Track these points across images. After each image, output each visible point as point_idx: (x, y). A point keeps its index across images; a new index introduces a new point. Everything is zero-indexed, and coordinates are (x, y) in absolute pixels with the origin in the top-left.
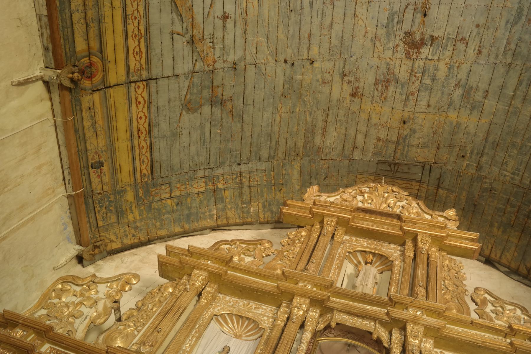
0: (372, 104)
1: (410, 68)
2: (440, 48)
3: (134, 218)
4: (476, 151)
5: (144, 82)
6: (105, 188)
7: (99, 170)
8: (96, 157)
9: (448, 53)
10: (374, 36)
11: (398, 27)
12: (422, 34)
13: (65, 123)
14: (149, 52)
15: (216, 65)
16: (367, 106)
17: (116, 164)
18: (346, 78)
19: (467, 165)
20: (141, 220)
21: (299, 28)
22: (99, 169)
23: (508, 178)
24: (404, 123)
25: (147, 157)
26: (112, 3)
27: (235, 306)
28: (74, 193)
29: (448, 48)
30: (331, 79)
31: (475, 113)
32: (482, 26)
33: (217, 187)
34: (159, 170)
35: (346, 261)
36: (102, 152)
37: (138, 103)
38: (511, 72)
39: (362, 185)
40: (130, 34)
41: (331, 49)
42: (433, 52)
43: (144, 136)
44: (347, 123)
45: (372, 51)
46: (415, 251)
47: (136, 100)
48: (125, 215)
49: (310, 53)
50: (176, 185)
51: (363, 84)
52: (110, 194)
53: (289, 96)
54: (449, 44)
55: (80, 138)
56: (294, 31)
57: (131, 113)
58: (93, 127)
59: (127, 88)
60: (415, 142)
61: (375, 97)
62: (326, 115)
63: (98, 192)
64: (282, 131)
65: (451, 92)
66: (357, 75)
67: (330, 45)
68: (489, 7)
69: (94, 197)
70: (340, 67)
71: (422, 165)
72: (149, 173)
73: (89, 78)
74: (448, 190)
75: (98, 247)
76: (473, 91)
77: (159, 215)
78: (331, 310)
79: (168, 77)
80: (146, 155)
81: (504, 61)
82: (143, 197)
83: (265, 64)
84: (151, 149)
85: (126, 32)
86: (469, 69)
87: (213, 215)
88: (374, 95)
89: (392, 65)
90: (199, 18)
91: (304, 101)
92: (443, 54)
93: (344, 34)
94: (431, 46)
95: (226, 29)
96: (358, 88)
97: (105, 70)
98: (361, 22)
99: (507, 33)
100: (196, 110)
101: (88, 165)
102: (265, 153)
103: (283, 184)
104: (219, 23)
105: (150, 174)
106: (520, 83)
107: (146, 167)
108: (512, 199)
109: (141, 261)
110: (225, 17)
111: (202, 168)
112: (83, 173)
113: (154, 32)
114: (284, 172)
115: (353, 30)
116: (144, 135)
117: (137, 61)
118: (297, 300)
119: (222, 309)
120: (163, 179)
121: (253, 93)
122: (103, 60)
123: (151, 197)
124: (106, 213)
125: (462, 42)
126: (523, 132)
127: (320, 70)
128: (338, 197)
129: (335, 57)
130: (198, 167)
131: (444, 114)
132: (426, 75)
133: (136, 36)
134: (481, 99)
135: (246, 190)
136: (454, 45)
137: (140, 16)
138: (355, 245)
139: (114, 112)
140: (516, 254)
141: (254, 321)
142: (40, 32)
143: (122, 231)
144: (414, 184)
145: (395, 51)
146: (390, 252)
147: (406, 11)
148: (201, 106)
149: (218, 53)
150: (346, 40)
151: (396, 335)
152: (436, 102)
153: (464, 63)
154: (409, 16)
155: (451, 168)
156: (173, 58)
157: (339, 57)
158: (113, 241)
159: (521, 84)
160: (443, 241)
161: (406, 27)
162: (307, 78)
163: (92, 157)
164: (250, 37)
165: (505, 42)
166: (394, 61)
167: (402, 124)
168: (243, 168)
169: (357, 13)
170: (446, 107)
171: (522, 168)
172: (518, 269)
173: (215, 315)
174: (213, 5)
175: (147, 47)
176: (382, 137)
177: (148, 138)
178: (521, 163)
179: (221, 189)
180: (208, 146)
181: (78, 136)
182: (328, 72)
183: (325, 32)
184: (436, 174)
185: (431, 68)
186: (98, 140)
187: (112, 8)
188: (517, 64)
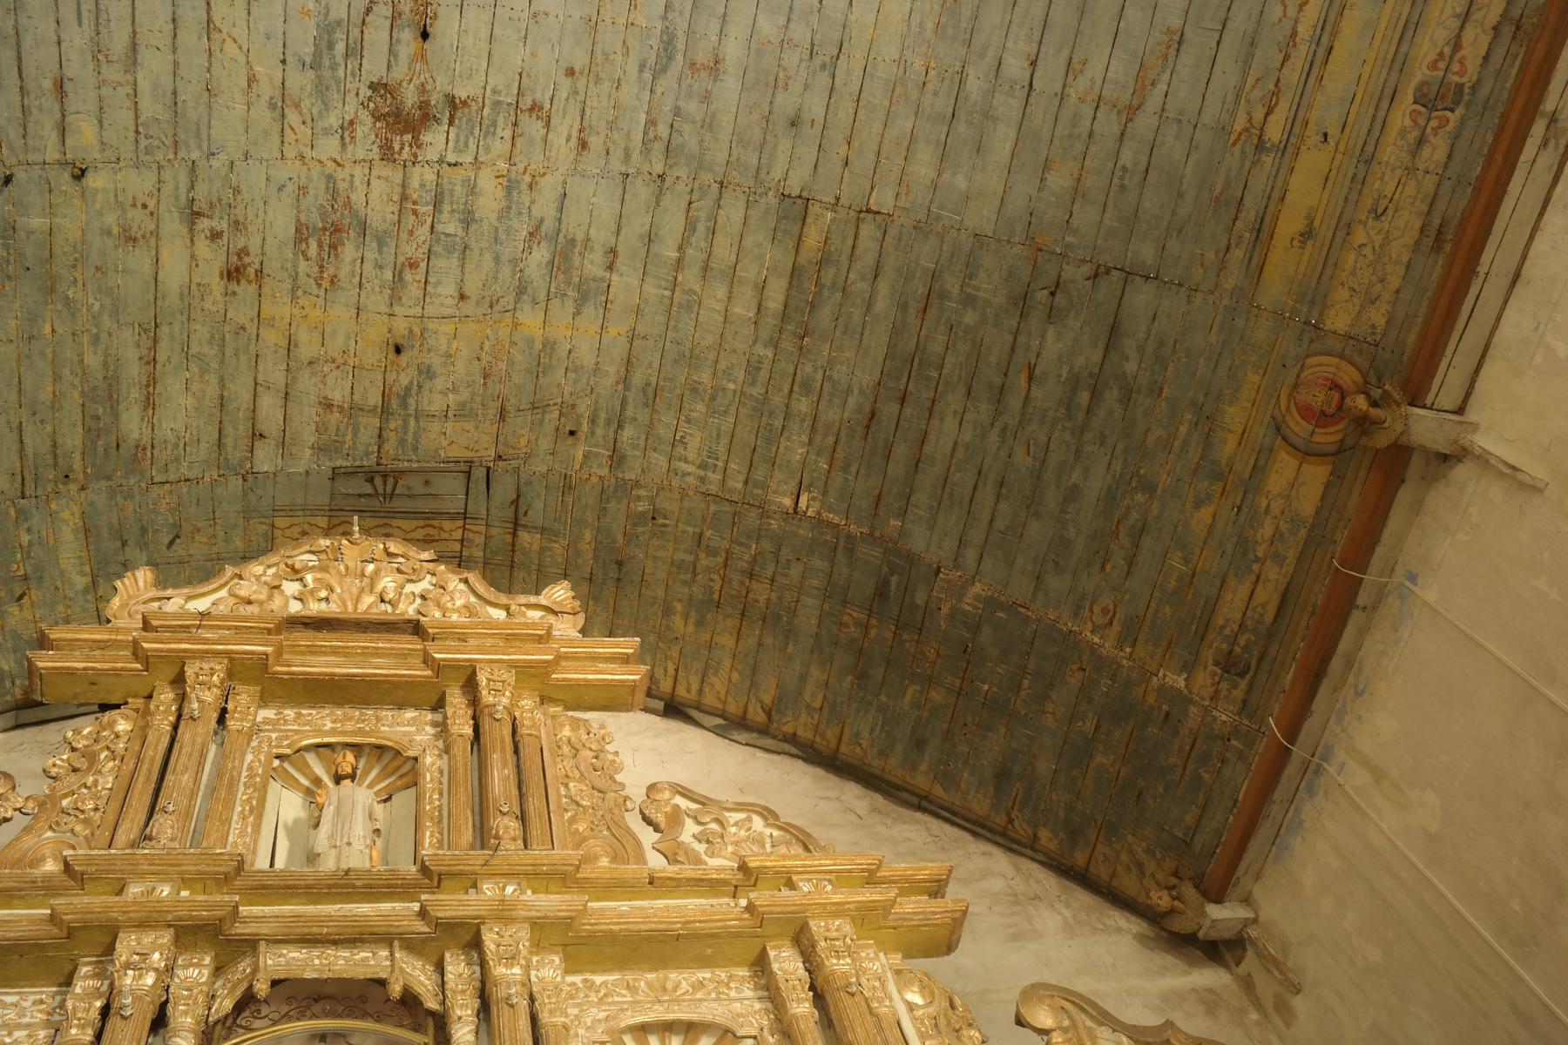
0: (294, 299)
1: (398, 190)
2: (477, 132)
4: (603, 415)
9: (499, 146)
10: (278, 93)
11: (349, 66)
12: (422, 89)
16: (279, 307)
18: (204, 224)
23: (690, 479)
24: (398, 350)
29: (499, 132)
30: (152, 227)
31: (591, 312)
32: (581, 73)
35: (275, 787)
38: (667, 200)
39: (294, 549)
41: (141, 129)
42: (457, 141)
44: (222, 362)
45: (276, 140)
46: (474, 718)
49: (69, 142)
54: (501, 120)
60: (437, 404)
61: (302, 279)
62: (150, 343)
65: (520, 255)
66: (237, 211)
67: (137, 117)
68: (593, 23)
70: (177, 188)
71: (464, 467)
74: (543, 530)
76: (576, 251)
78: (250, 945)
81: (646, 168)
86: (561, 190)
88: (297, 273)
89: (344, 180)
91: (67, 302)
92: (488, 150)
93: (180, 86)
94: (451, 124)
96: (244, 252)
98: (231, 48)
99: (646, 95)
103: (26, 578)
106: (690, 226)
108: (708, 533)
114: (25, 538)
115: (209, 71)
118: (127, 946)
125: (534, 116)
126: (712, 356)
127: (112, 200)
128: (223, 593)
129: (160, 157)
132: (446, 207)
134: (600, 273)
136: (515, 125)
138: (296, 732)
140: (735, 676)
144: (447, 525)
145: (348, 139)
146: (405, 734)
147: (368, 19)
150: (190, 104)
151: (458, 968)
152: (480, 286)
153: (545, 174)
154: (377, 35)
157: (171, 156)
159: (695, 230)
160: (548, 674)
161: (374, 67)
165: (643, 117)
166: (348, 170)
167: (392, 355)
169: (216, 18)
170: (509, 300)
171: (722, 449)
176: (337, 396)
178: (718, 435)
182: (139, 205)
183: (112, 73)
184: (504, 490)
185: (458, 188)
188: (678, 178)
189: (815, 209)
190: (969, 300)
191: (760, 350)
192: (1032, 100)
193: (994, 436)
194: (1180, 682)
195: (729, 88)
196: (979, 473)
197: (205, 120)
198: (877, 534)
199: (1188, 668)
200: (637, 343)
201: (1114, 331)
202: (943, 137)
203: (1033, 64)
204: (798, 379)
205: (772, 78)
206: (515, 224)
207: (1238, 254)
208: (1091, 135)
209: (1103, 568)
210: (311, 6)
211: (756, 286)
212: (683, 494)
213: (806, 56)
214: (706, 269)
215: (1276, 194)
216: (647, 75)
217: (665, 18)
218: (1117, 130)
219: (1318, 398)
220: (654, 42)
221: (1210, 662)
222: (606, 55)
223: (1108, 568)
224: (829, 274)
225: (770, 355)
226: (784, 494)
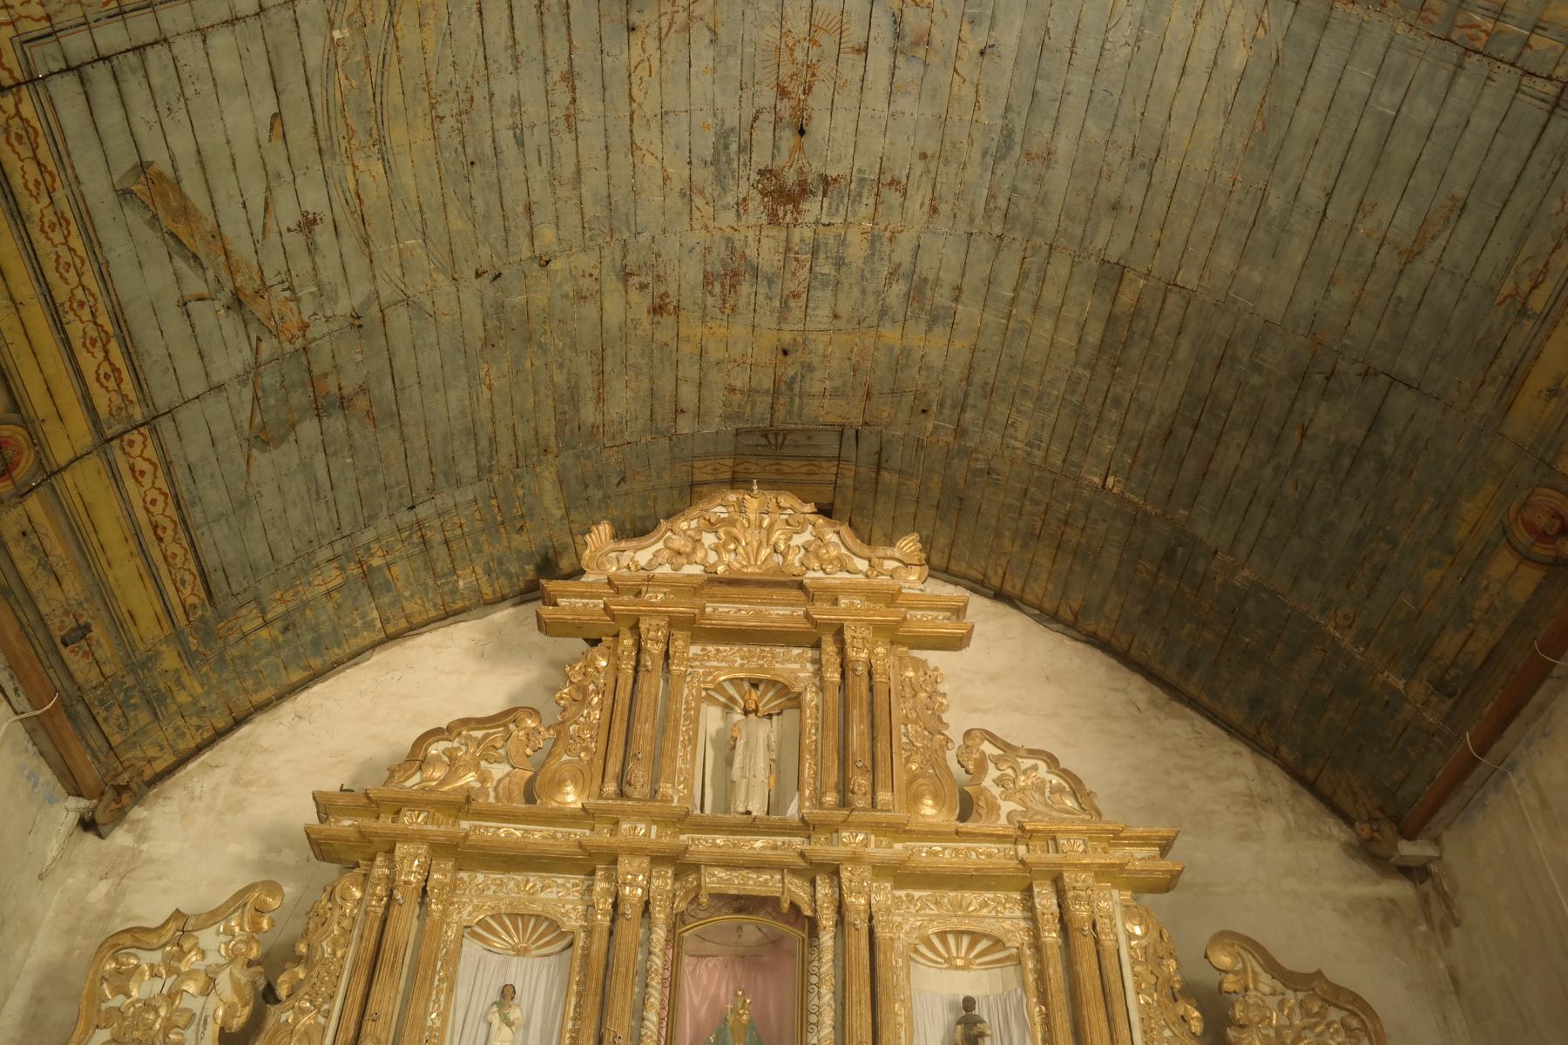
0: (704, 322)
1: (783, 244)
3: (192, 695)
4: (949, 402)
5: (142, 430)
6: (108, 670)
7: (83, 643)
9: (864, 211)
10: (686, 185)
12: (801, 171)
14: (136, 363)
15: (309, 334)
16: (692, 328)
18: (635, 280)
19: (935, 428)
20: (208, 693)
21: (497, 195)
23: (1019, 452)
24: (785, 353)
27: (501, 894)
29: (864, 200)
30: (597, 287)
31: (939, 331)
32: (933, 157)
33: (370, 567)
34: (224, 585)
35: (704, 706)
37: (137, 475)
38: (1004, 254)
39: (709, 503)
40: (77, 343)
44: (651, 367)
46: (842, 666)
47: (132, 469)
48: (169, 701)
51: (676, 287)
52: (123, 677)
53: (501, 343)
54: (865, 192)
56: (487, 204)
58: (44, 567)
59: (102, 455)
60: (817, 387)
61: (710, 309)
62: (599, 362)
63: (94, 684)
64: (498, 416)
68: (942, 120)
69: (86, 699)
71: (840, 429)
74: (900, 472)
75: (127, 788)
77: (247, 665)
78: (696, 867)
79: (197, 397)
81: (987, 229)
82: (201, 649)
83: (430, 292)
84: (195, 551)
85: (66, 341)
87: (373, 620)
90: (242, 248)
91: (540, 345)
92: (855, 214)
93: (612, 190)
94: (824, 195)
95: (316, 249)
96: (666, 295)
97: (37, 441)
98: (649, 160)
99: (988, 175)
100: (282, 439)
101: (54, 644)
102: (467, 468)
103: (522, 516)
104: (296, 241)
106: (1024, 275)
108: (1033, 490)
109: (236, 781)
110: (308, 224)
111: (325, 542)
112: (47, 664)
113: (137, 315)
114: (520, 492)
116: (170, 532)
118: (625, 864)
119: (477, 908)
121: (413, 360)
122: (25, 423)
126: (1039, 369)
128: (660, 545)
129: (600, 241)
130: (315, 544)
131: (873, 332)
132: (822, 255)
133: (93, 342)
134: (948, 303)
135: (439, 552)
137: (93, 295)
138: (717, 668)
139: (85, 518)
140: (1050, 586)
141: (546, 919)
143: (170, 730)
144: (825, 464)
145: (742, 211)
146: (793, 671)
148: (293, 426)
149: (308, 308)
151: (824, 890)
154: (763, 134)
155: (900, 433)
156: (200, 352)
157: (608, 239)
158: (155, 758)
160: (897, 629)
161: (761, 158)
162: (540, 298)
163: (58, 625)
164: (379, 248)
165: (985, 192)
167: (780, 356)
168: (422, 511)
169: (638, 142)
170: (874, 319)
171: (1045, 435)
172: (1057, 611)
173: (466, 927)
174: (271, 208)
175: (129, 354)
176: (739, 384)
177: (181, 534)
178: (1043, 425)
179: (379, 568)
180: (330, 497)
181: (12, 601)
184: (870, 444)
185: (831, 241)
187: (15, 305)
189: (1129, 275)
190: (1257, 368)
191: (1080, 370)
192: (1324, 225)
193: (1269, 470)
194: (1400, 684)
195: (1059, 175)
196: (1255, 493)
197: (632, 211)
198: (1168, 516)
199: (1409, 676)
200: (978, 354)
201: (1376, 421)
202: (1243, 240)
203: (1329, 195)
204: (1110, 395)
205: (1097, 170)
206: (878, 266)
207: (1490, 390)
208: (1373, 265)
209: (1348, 586)
210: (710, 121)
211: (1078, 324)
212: (1013, 462)
213: (1128, 156)
214: (1036, 307)
215: (1531, 353)
216: (989, 161)
217: (1005, 117)
218: (1397, 267)
219: (1542, 521)
220: (996, 135)
221: (1425, 679)
222: (954, 145)
223: (1352, 588)
224: (1140, 325)
225: (1088, 375)
226: (1095, 474)
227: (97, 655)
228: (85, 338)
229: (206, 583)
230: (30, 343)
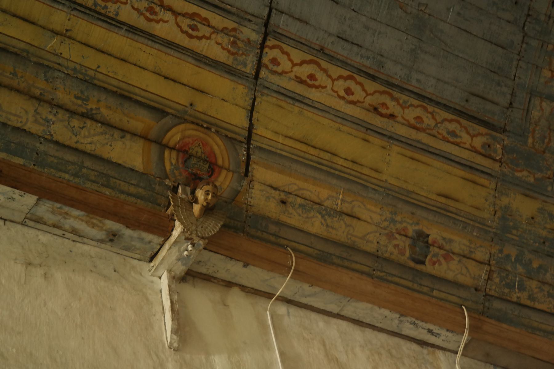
5: (268, 43)
6: (481, 254)
7: (434, 250)
8: (401, 241)
13: (299, 275)
17: (432, 203)
22: (431, 248)
25: (445, 120)
26: (52, 31)
28: (466, 333)
36: (393, 221)
40: (141, 23)
43: (394, 103)
47: (301, 82)
50: (542, 80)
52: (501, 251)
55: (343, 258)
57: (327, 109)
58: (330, 215)
59: (266, 91)
63: (484, 276)
69: (492, 293)
72: (487, 134)
73: (213, 171)
80: (439, 120)
82: (539, 175)
84: (431, 100)
85: (133, 30)
105: (490, 132)
107: (468, 133)
112: (425, 289)
116: (391, 104)
117: (213, 36)
120: (514, 105)
123: (547, 155)
124: (544, 283)
133: (151, 10)
139: (312, 151)
142: (68, 235)
163: (396, 251)
177: (403, 98)
181: (336, 260)
186: (363, 217)
187: (65, 36)
227: (456, 250)
228: (142, 14)
229: (472, 118)
230: (110, 55)
